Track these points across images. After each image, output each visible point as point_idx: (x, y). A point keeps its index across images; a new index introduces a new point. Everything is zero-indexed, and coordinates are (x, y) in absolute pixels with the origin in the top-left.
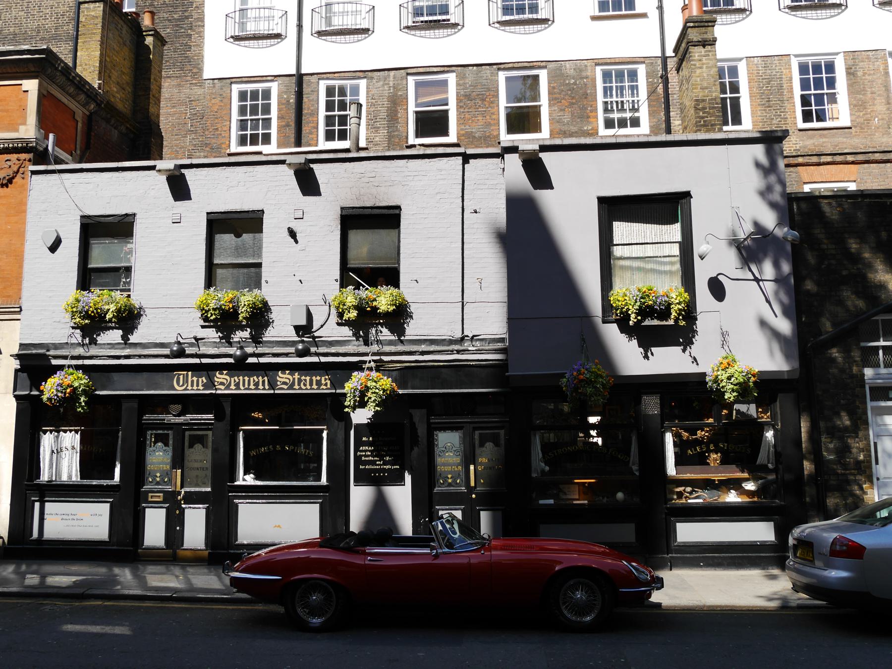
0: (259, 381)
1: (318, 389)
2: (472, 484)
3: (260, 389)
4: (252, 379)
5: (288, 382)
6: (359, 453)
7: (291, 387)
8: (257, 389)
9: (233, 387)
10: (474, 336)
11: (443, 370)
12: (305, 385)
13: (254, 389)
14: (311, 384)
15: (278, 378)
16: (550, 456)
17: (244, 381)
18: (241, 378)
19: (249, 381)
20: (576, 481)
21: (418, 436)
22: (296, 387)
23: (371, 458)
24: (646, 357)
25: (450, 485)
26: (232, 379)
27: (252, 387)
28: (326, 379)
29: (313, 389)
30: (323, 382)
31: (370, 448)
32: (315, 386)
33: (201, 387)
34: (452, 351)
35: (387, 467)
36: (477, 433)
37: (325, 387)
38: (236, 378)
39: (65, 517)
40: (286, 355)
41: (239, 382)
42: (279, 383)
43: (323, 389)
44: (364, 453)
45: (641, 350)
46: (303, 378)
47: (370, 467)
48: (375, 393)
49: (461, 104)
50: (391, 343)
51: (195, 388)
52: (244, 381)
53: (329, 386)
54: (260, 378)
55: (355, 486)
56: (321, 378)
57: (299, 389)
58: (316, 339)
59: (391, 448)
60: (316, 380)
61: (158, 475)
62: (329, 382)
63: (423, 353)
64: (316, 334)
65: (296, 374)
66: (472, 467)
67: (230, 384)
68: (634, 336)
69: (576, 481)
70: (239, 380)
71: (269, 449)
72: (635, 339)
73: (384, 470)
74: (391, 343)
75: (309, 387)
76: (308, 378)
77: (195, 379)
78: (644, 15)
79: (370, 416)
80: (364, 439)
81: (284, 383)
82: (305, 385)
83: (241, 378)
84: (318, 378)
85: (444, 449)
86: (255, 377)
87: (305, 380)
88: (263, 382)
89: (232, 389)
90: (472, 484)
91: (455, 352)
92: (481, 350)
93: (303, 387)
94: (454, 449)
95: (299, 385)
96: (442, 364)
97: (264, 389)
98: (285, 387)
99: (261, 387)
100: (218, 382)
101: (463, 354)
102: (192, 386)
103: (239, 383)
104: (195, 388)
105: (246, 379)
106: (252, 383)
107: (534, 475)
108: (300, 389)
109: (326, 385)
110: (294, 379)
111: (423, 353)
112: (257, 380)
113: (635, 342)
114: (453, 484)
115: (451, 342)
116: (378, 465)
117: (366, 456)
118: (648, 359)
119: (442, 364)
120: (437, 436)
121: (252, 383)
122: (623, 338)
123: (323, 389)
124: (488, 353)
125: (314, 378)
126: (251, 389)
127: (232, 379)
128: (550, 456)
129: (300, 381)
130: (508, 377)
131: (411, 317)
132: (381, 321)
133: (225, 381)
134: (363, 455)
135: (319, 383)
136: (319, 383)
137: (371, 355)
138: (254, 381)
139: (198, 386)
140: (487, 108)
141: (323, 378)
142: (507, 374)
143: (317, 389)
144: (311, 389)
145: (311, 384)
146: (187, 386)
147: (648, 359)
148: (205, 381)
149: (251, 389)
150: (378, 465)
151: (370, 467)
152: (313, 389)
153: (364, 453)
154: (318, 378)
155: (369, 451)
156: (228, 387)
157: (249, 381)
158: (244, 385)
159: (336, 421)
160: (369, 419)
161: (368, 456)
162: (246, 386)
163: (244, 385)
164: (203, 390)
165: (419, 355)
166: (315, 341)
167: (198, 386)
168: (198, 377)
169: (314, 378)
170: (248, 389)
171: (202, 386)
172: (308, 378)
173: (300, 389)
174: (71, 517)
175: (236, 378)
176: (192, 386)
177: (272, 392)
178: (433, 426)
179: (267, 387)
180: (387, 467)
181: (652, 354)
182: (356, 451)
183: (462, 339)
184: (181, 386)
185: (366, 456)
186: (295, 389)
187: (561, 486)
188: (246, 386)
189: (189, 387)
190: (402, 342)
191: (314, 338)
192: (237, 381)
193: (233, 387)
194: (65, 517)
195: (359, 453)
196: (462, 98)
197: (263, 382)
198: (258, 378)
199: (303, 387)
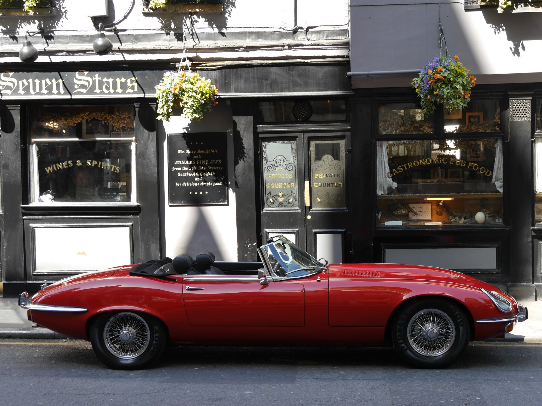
0: (52, 85)
1: (123, 93)
2: (307, 203)
3: (53, 94)
4: (43, 82)
6: (174, 169)
7: (91, 90)
8: (50, 93)
9: (21, 91)
10: (309, 28)
11: (272, 69)
12: (107, 88)
13: (47, 94)
14: (115, 88)
15: (75, 81)
16: (398, 171)
17: (34, 84)
18: (31, 81)
19: (40, 84)
20: (428, 199)
21: (244, 147)
22: (97, 90)
23: (188, 174)
24: (516, 52)
25: (281, 204)
26: (20, 82)
27: (44, 91)
28: (132, 82)
29: (118, 93)
30: (129, 85)
31: (187, 163)
32: (119, 90)
34: (283, 46)
35: (207, 184)
36: (313, 144)
37: (131, 91)
38: (24, 81)
40: (84, 52)
42: (76, 86)
43: (129, 93)
44: (180, 169)
45: (511, 44)
46: (105, 80)
47: (188, 184)
48: (191, 97)
50: (209, 37)
52: (34, 84)
53: (136, 90)
54: (54, 81)
55: (170, 206)
56: (126, 81)
57: (100, 93)
58: (119, 33)
59: (212, 162)
60: (121, 82)
62: (136, 84)
63: (248, 49)
64: (118, 27)
65: (97, 75)
66: (307, 184)
67: (93, 87)
68: (502, 27)
69: (428, 199)
70: (29, 83)
71: (68, 164)
72: (503, 30)
73: (204, 188)
74: (209, 37)
75: (112, 91)
76: (111, 80)
79: (186, 125)
80: (180, 152)
81: (83, 86)
82: (107, 88)
83: (31, 81)
84: (123, 80)
85: (274, 163)
86: (47, 80)
87: (108, 83)
88: (58, 85)
89: (20, 94)
90: (307, 203)
91: (286, 47)
92: (318, 45)
93: (106, 92)
94: (286, 162)
95: (100, 88)
96: (270, 62)
97: (59, 93)
98: (84, 91)
99: (55, 91)
100: (78, 85)
101: (296, 50)
103: (28, 87)
105: (37, 81)
106: (44, 87)
107: (379, 192)
108: (102, 93)
110: (94, 81)
111: (248, 49)
112: (49, 83)
113: (503, 34)
114: (285, 203)
115: (282, 35)
116: (197, 182)
117: (182, 172)
118: (519, 55)
119: (270, 62)
120: (265, 147)
121: (44, 87)
122: (489, 28)
123: (129, 93)
124: (326, 49)
125: (118, 80)
126: (43, 94)
127: (20, 82)
128: (398, 171)
129: (101, 83)
130: (350, 77)
131: (233, 5)
132: (198, 10)
133: (11, 85)
134: (178, 171)
135: (124, 86)
136: (124, 86)
137: (186, 52)
138: (46, 84)
141: (129, 80)
142: (348, 73)
143: (122, 93)
144: (115, 93)
145: (115, 88)
147: (519, 55)
149: (43, 94)
150: (197, 182)
151: (188, 184)
152: (118, 93)
153: (180, 169)
154: (123, 80)
155: (186, 166)
157: (40, 84)
158: (34, 89)
159: (146, 131)
160: (186, 128)
161: (185, 172)
162: (38, 91)
163: (34, 89)
165: (244, 51)
166: (118, 36)
168: (40, 79)
169: (118, 80)
170: (40, 94)
171: (46, 89)
173: (102, 93)
175: (24, 81)
177: (68, 97)
178: (260, 136)
179: (62, 91)
180: (207, 184)
181: (524, 48)
182: (171, 165)
183: (295, 31)
185: (182, 172)
186: (96, 94)
187: (411, 206)
188: (38, 91)
190: (223, 34)
191: (116, 31)
192: (26, 84)
193: (21, 91)
195: (174, 169)
197: (58, 85)
198: (51, 81)
199: (106, 92)
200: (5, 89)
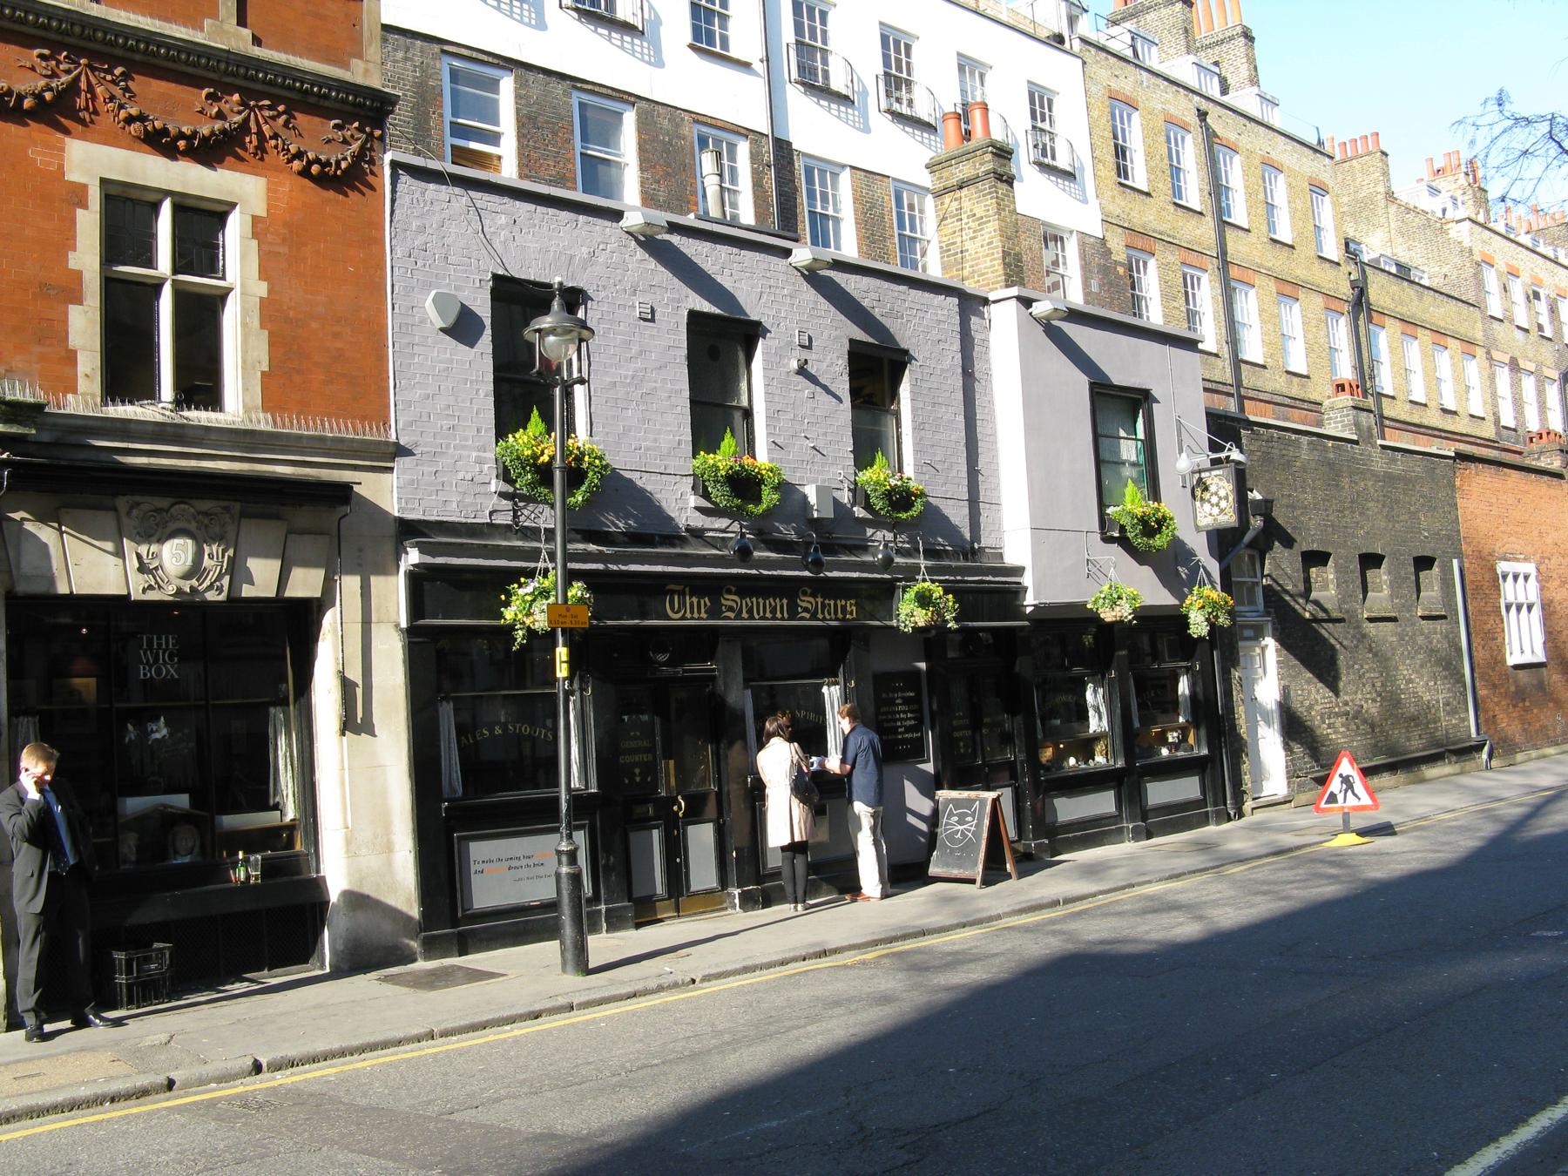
5: (810, 607)
6: (880, 718)
8: (774, 618)
9: (745, 615)
12: (829, 614)
17: (758, 604)
22: (820, 616)
27: (768, 615)
33: (704, 615)
35: (910, 735)
39: (514, 863)
41: (752, 606)
46: (827, 602)
49: (525, 131)
51: (696, 615)
52: (758, 604)
54: (778, 600)
61: (637, 771)
62: (854, 608)
70: (752, 603)
76: (832, 602)
77: (695, 600)
78: (745, 66)
82: (829, 614)
84: (843, 602)
86: (771, 600)
87: (829, 605)
95: (823, 613)
97: (783, 619)
99: (779, 615)
102: (692, 612)
104: (696, 615)
109: (851, 613)
110: (817, 603)
139: (699, 612)
140: (560, 148)
146: (685, 612)
148: (708, 604)
156: (738, 616)
158: (758, 614)
162: (761, 614)
163: (758, 613)
164: (707, 619)
167: (699, 612)
172: (832, 602)
174: (524, 862)
176: (692, 612)
179: (786, 615)
180: (910, 735)
184: (676, 613)
188: (761, 614)
189: (688, 615)
194: (514, 863)
195: (880, 718)
196: (524, 120)
199: (828, 617)
200: (728, 611)
